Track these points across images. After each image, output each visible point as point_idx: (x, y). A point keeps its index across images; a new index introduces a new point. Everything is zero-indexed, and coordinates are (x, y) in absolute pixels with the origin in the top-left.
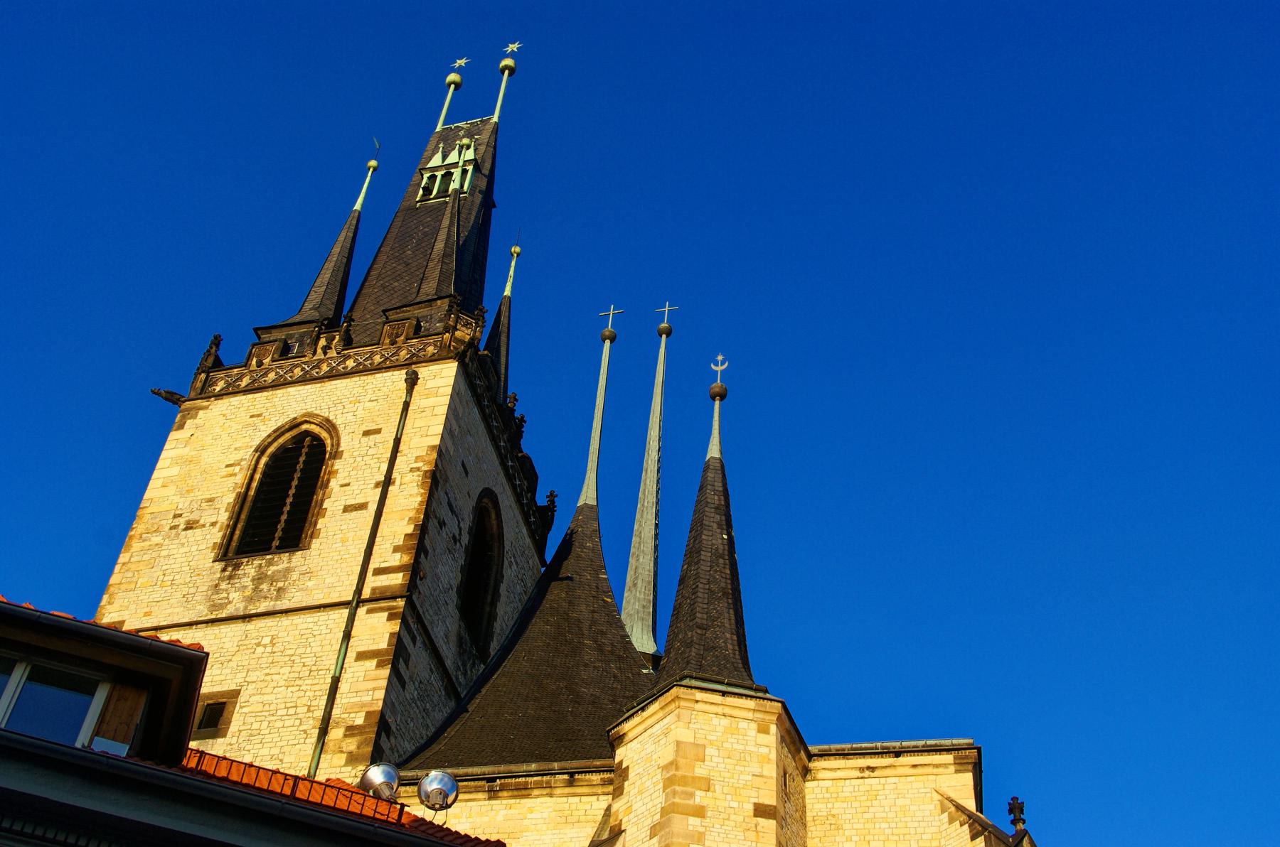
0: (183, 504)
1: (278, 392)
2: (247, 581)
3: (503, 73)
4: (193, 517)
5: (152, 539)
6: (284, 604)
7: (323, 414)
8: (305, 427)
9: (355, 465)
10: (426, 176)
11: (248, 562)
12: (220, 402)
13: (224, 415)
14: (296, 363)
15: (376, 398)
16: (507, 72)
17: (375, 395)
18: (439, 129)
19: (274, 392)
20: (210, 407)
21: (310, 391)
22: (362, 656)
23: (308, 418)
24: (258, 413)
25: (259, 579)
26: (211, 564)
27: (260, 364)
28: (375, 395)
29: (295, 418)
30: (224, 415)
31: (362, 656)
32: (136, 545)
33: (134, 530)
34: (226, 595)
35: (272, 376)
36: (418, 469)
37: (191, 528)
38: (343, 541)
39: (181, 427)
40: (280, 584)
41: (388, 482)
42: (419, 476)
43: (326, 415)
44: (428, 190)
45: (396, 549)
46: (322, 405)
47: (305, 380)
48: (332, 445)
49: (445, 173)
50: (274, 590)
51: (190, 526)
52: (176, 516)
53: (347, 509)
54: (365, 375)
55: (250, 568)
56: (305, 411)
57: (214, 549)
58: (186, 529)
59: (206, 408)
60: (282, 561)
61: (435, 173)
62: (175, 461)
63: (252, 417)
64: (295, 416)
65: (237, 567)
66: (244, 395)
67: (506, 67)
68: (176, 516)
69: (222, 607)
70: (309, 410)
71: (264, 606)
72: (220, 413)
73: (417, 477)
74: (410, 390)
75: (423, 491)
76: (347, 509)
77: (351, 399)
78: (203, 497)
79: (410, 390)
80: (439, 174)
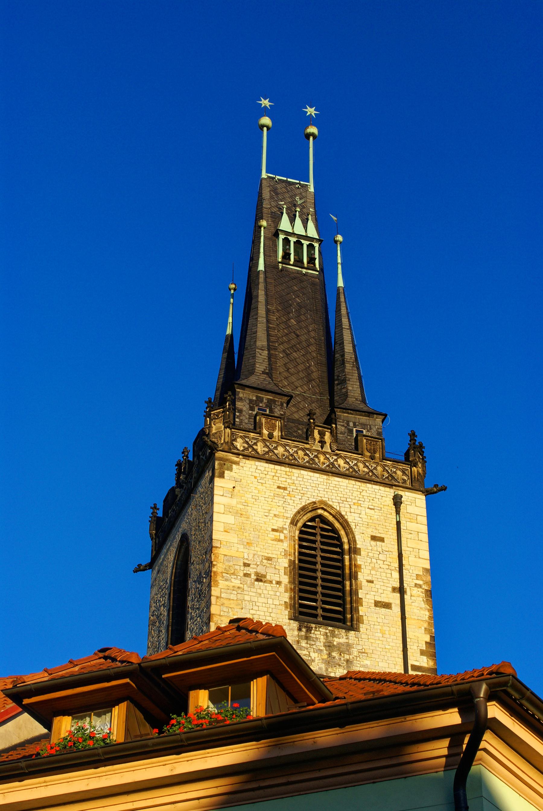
0: (247, 554)
1: (294, 470)
2: (320, 645)
3: (309, 139)
4: (261, 570)
5: (233, 580)
7: (335, 507)
8: (320, 512)
9: (372, 565)
10: (282, 237)
11: (316, 628)
12: (247, 462)
13: (255, 477)
14: (301, 446)
15: (372, 507)
16: (311, 138)
17: (370, 504)
18: (264, 175)
19: (291, 470)
20: (241, 464)
21: (319, 479)
23: (325, 506)
24: (283, 486)
25: (329, 646)
26: (288, 621)
27: (271, 436)
28: (370, 504)
29: (314, 503)
30: (255, 477)
32: (222, 583)
33: (216, 567)
34: (308, 654)
35: (281, 450)
36: (420, 586)
37: (261, 581)
38: (383, 634)
39: (222, 476)
40: (347, 657)
41: (401, 590)
42: (422, 592)
43: (338, 509)
44: (286, 256)
45: (422, 653)
46: (333, 497)
48: (349, 543)
49: (297, 240)
50: (344, 660)
51: (260, 578)
52: (246, 565)
54: (359, 481)
56: (320, 498)
57: (286, 607)
58: (257, 580)
59: (237, 463)
61: (289, 237)
62: (229, 510)
63: (279, 487)
64: (314, 500)
65: (309, 630)
66: (266, 463)
67: (313, 134)
68: (246, 565)
70: (324, 499)
72: (250, 473)
74: (398, 512)
75: (429, 608)
77: (354, 501)
78: (263, 554)
79: (398, 512)
80: (293, 240)
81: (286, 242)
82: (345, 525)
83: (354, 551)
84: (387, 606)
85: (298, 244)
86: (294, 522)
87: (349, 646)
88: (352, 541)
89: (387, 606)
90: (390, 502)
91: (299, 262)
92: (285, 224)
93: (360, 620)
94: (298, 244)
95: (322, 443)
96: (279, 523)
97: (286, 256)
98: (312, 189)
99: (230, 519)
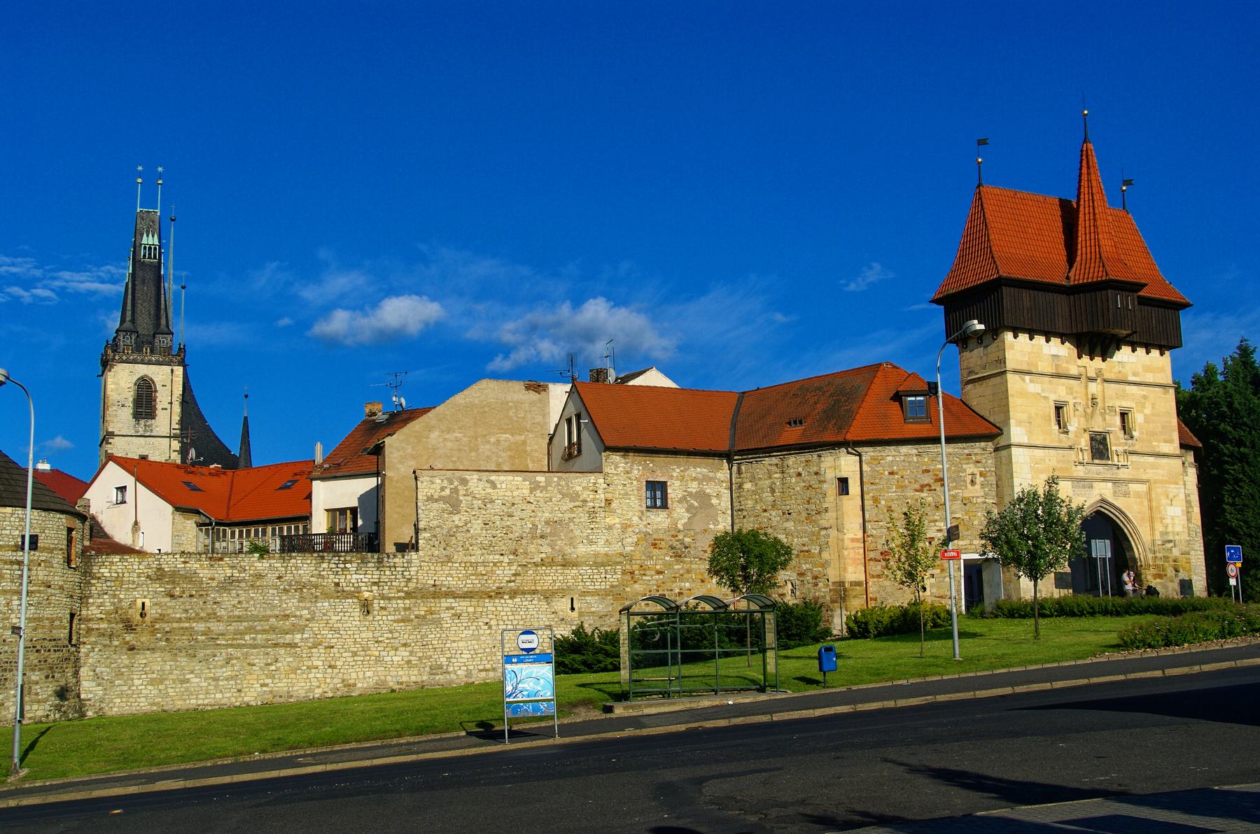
2: (142, 426)
6: (153, 434)
22: (174, 451)
25: (145, 426)
31: (174, 451)
41: (171, 403)
44: (145, 256)
47: (143, 363)
51: (123, 406)
53: (163, 409)
55: (142, 422)
60: (150, 422)
69: (138, 432)
71: (148, 434)
73: (177, 403)
76: (163, 409)
80: (147, 246)
81: (145, 248)
82: (153, 382)
83: (156, 391)
84: (166, 409)
85: (150, 248)
86: (135, 384)
87: (152, 425)
88: (156, 388)
89: (166, 409)
90: (170, 371)
91: (150, 258)
92: (144, 241)
93: (156, 415)
94: (150, 248)
95: (146, 353)
96: (129, 385)
97: (145, 256)
98: (159, 214)
99: (113, 386)
